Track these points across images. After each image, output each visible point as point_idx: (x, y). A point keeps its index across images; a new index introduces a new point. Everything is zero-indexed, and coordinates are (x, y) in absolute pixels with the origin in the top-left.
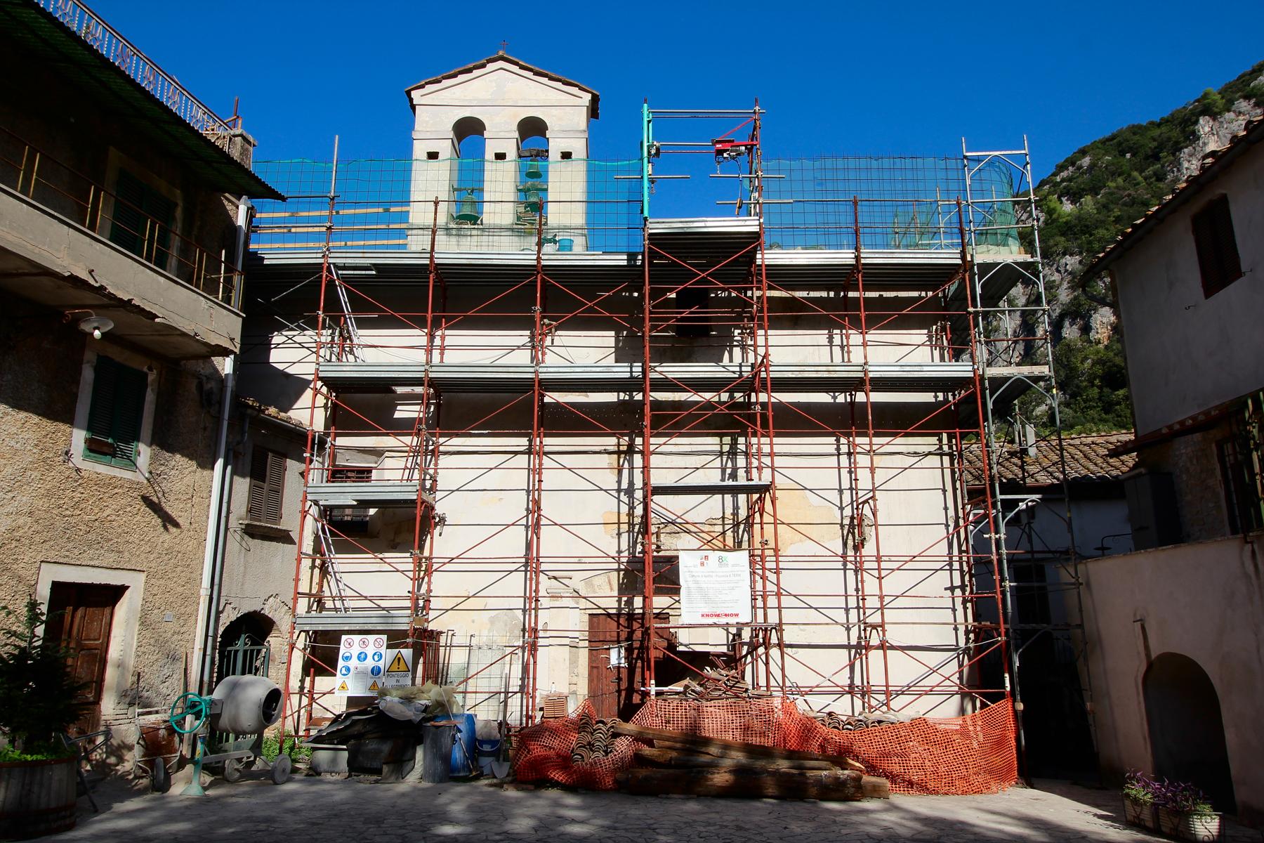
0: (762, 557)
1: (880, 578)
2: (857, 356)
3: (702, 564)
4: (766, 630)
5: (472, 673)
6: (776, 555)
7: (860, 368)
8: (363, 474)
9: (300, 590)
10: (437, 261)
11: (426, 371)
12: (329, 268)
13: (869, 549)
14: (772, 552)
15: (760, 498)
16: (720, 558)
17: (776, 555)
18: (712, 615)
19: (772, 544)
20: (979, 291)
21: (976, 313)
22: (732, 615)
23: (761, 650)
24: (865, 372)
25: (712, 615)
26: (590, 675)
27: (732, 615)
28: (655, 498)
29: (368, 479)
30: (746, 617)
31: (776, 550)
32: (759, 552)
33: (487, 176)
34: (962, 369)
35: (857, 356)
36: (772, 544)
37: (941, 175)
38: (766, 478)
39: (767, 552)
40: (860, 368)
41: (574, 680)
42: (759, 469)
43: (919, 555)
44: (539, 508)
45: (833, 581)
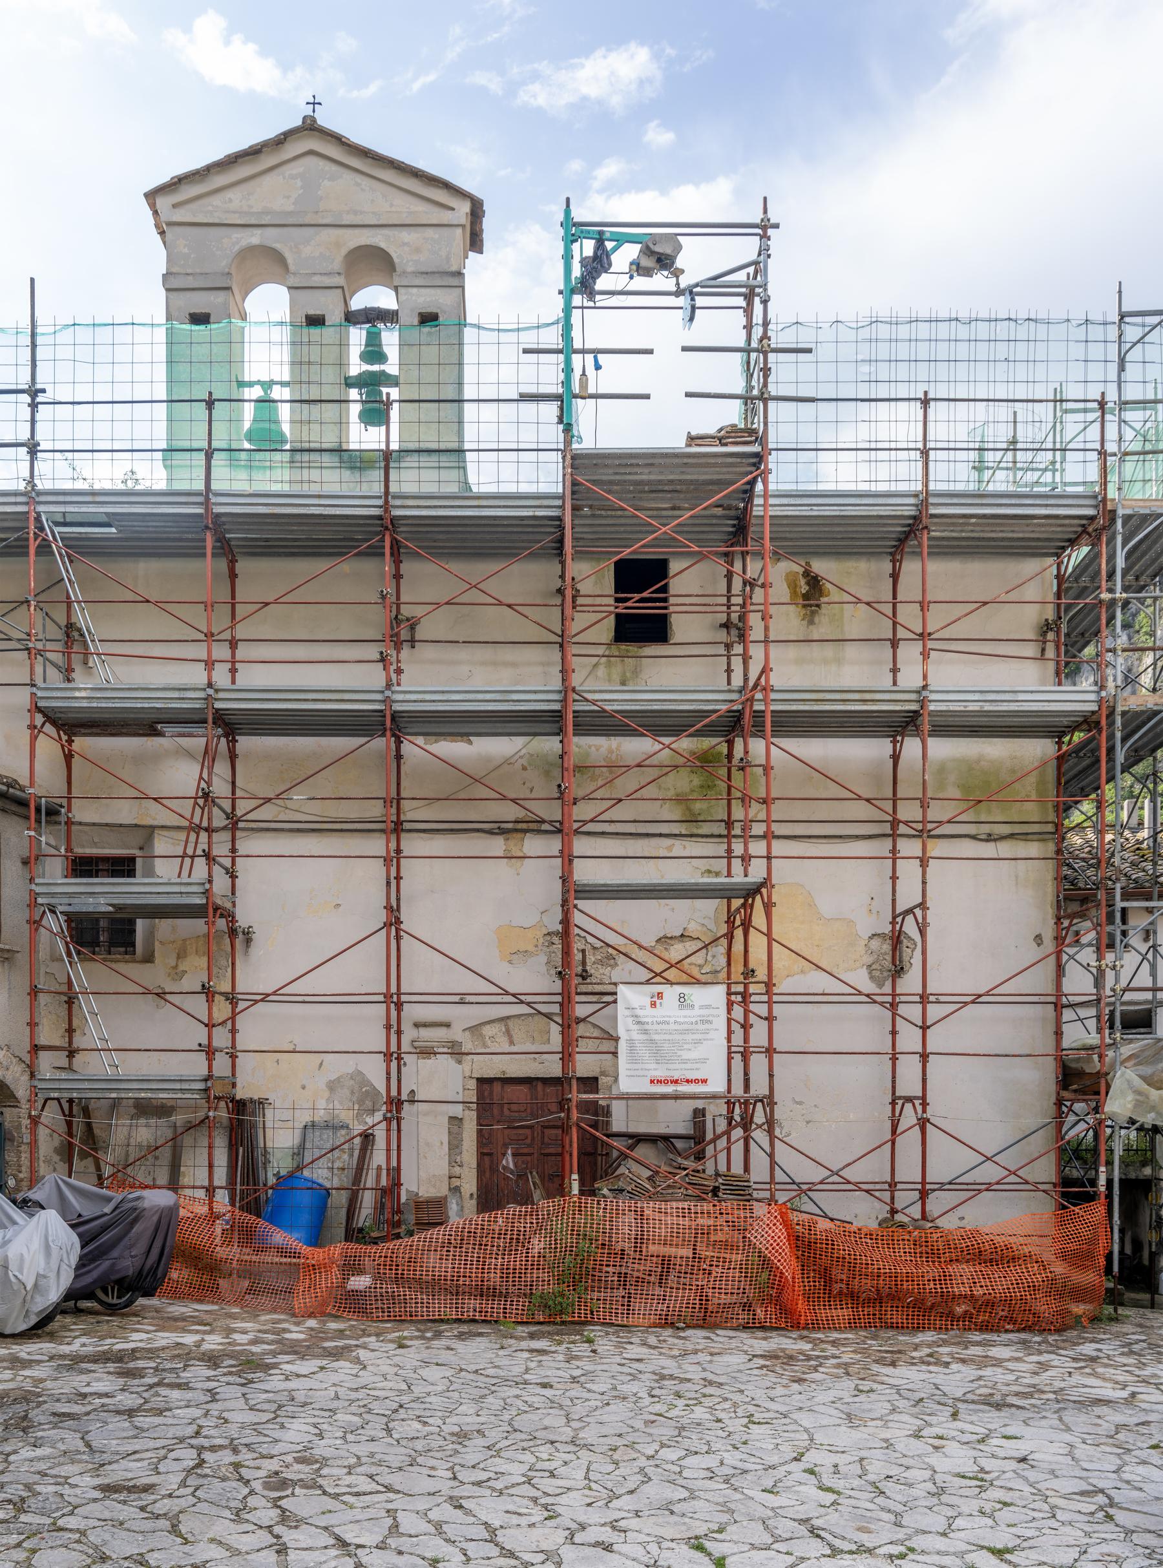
0: (745, 996)
1: (924, 1028)
2: (910, 678)
3: (653, 1005)
4: (746, 1103)
5: (307, 1160)
6: (768, 992)
7: (913, 696)
8: (123, 867)
9: (42, 1040)
10: (218, 510)
11: (207, 698)
12: (38, 519)
13: (910, 983)
14: (761, 988)
15: (744, 905)
16: (682, 997)
17: (768, 992)
18: (666, 1082)
19: (761, 974)
20: (1120, 563)
21: (1113, 602)
22: (696, 1081)
23: (738, 1133)
24: (923, 702)
25: (666, 1082)
26: (479, 1165)
27: (696, 1081)
28: (581, 904)
29: (131, 873)
30: (717, 1085)
31: (769, 985)
32: (740, 988)
34: (1079, 696)
35: (910, 678)
36: (761, 974)
37: (1077, 351)
38: (757, 872)
39: (752, 989)
40: (913, 696)
41: (457, 1170)
42: (746, 859)
43: (987, 994)
44: (398, 921)
45: (864, 1027)
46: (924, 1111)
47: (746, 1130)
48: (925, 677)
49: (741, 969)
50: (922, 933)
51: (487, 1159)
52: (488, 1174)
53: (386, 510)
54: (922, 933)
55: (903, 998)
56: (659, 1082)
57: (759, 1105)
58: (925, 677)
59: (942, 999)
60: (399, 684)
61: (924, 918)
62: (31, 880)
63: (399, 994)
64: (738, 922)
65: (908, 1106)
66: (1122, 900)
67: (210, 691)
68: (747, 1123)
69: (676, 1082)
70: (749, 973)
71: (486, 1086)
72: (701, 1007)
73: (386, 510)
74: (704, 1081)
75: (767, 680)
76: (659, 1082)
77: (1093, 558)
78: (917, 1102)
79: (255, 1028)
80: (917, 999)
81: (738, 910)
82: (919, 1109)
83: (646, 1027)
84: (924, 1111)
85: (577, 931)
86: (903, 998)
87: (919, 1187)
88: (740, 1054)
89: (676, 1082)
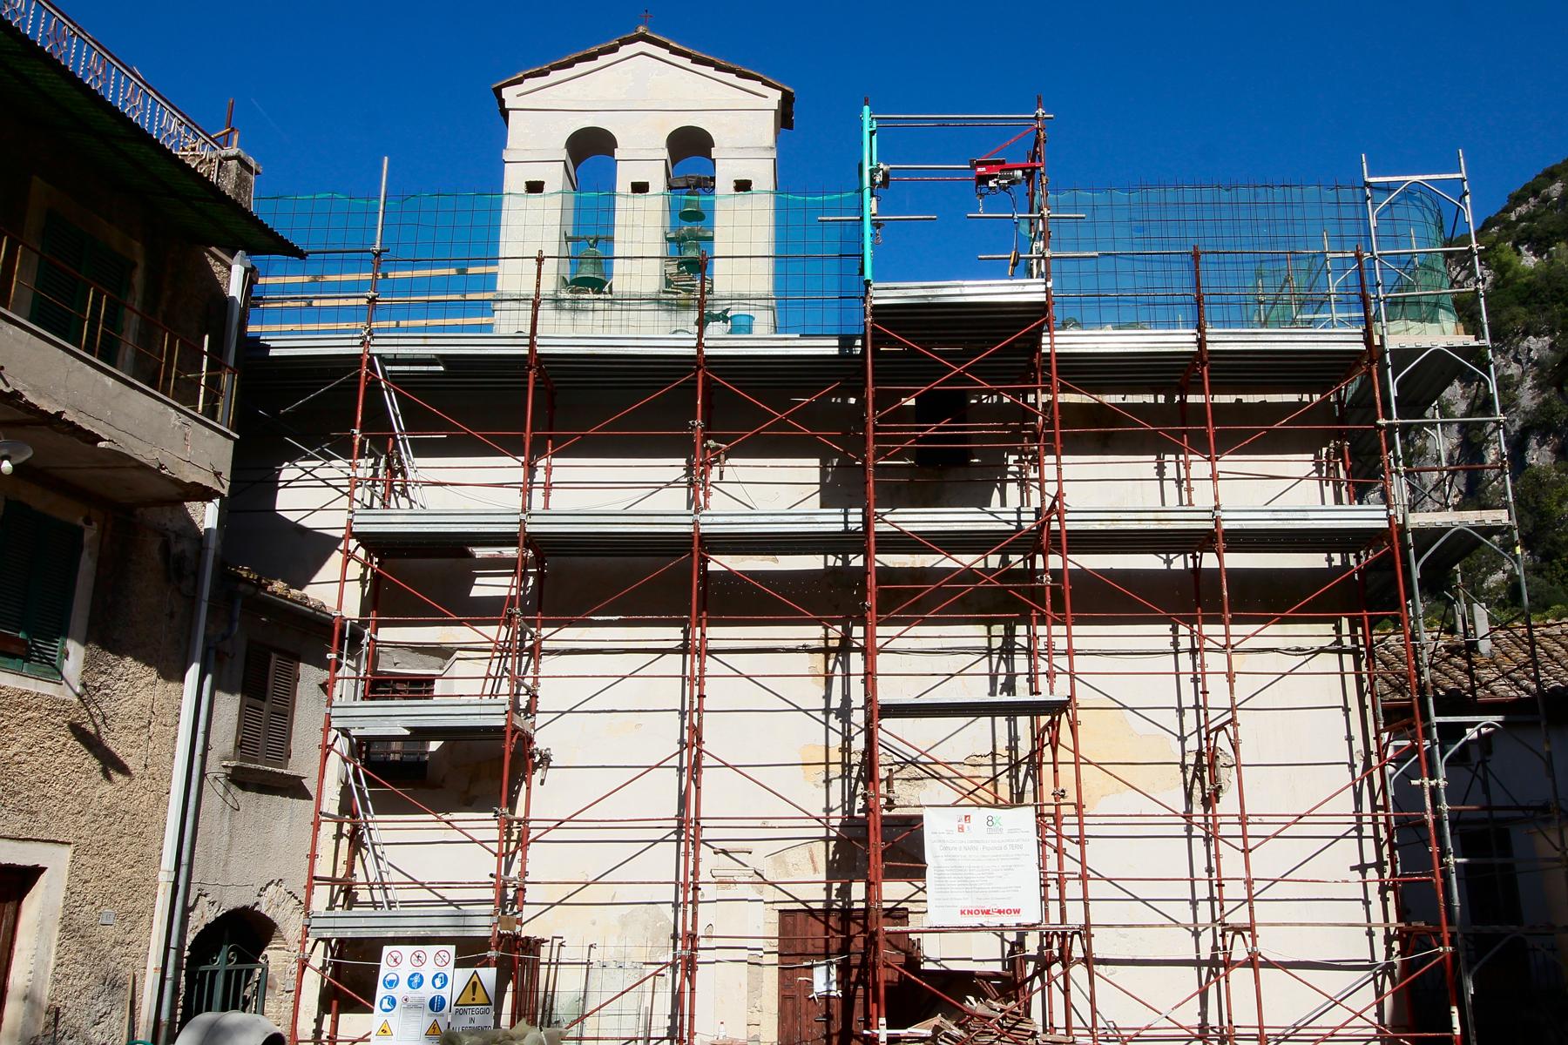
0: (1057, 818)
1: (1246, 851)
2: (1202, 496)
3: (961, 829)
4: (1064, 935)
5: (590, 1007)
6: (1079, 814)
7: (1208, 516)
8: (420, 687)
9: (317, 874)
10: (540, 350)
11: (522, 522)
12: (371, 362)
13: (1227, 804)
14: (1072, 810)
15: (1051, 722)
16: (990, 820)
17: (1079, 814)
18: (977, 912)
19: (1072, 796)
20: (1393, 392)
21: (1390, 429)
22: (1009, 911)
23: (1056, 969)
24: (1217, 521)
25: (977, 912)
26: (781, 1010)
27: (1009, 911)
28: (885, 723)
29: (428, 694)
30: (1031, 915)
31: (1079, 806)
32: (1051, 810)
33: (619, 218)
34: (1368, 516)
35: (1202, 496)
36: (1072, 796)
37: (1330, 212)
38: (1061, 692)
39: (1064, 810)
40: (1208, 516)
41: (756, 1018)
42: (1050, 675)
43: (1308, 814)
44: (700, 740)
45: (1170, 857)
46: (1254, 944)
47: (1064, 966)
48: (1216, 498)
49: (1052, 789)
50: (1235, 748)
51: (789, 1002)
52: (790, 1021)
53: (700, 351)
54: (1235, 748)
55: (1225, 819)
56: (970, 912)
57: (1076, 937)
58: (1216, 498)
59: (1266, 819)
60: (706, 506)
61: (1236, 735)
62: (329, 705)
63: (698, 818)
64: (1046, 740)
65: (1238, 938)
66: (1437, 715)
67: (523, 516)
68: (1066, 959)
69: (988, 912)
70: (1060, 795)
71: (789, 919)
72: (1010, 831)
73: (700, 351)
74: (1018, 911)
75: (1062, 504)
76: (970, 912)
77: (1367, 386)
78: (1246, 934)
79: (541, 861)
80: (1236, 819)
81: (1046, 728)
82: (1249, 941)
83: (954, 852)
84: (1254, 944)
85: (881, 750)
86: (1225, 819)
87: (1257, 1031)
88: (1050, 883)
89: (988, 912)
